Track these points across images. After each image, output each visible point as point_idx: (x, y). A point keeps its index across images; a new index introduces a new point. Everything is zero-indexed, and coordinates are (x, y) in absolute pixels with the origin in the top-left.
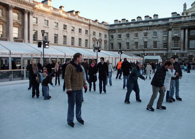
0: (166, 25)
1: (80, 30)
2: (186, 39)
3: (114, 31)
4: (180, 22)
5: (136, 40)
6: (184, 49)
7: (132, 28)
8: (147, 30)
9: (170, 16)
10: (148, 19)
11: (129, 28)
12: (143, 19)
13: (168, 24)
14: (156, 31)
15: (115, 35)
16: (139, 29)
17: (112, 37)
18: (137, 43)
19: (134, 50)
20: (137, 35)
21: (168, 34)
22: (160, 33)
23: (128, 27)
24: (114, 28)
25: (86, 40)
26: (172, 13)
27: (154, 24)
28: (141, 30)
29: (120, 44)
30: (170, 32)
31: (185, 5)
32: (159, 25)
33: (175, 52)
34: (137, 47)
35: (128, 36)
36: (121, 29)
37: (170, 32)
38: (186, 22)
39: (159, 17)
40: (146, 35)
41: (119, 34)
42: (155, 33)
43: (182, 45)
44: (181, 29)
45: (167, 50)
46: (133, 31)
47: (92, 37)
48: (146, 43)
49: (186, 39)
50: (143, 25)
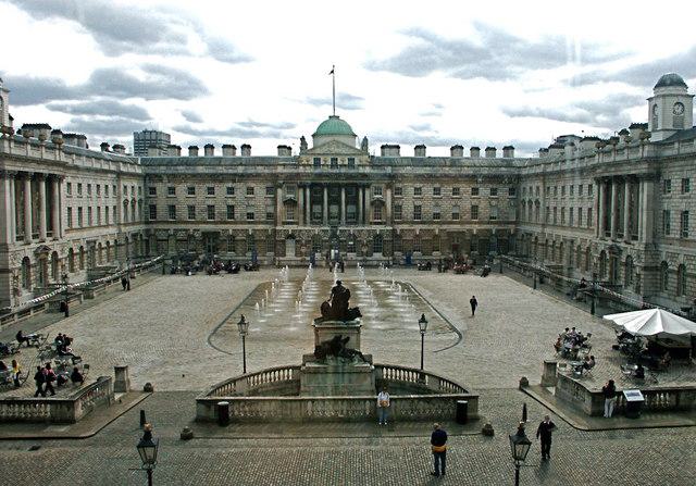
0: (273, 175)
1: (89, 185)
2: (308, 206)
3: (159, 177)
4: (298, 174)
5: (210, 202)
6: (305, 223)
7: (200, 175)
8: (234, 181)
9: (274, 153)
10: (159, 66)
11: (194, 175)
12: (218, 153)
13: (276, 176)
14: (253, 185)
15: (161, 188)
16: (218, 178)
17: (153, 190)
18: (211, 208)
19: (208, 223)
20: (211, 191)
21: (275, 193)
22: (260, 190)
23: (190, 172)
24: (157, 171)
25: (115, 207)
26: (279, 147)
27: (249, 172)
28: (221, 182)
29: (172, 209)
30: (280, 191)
31: (303, 139)
32: (258, 175)
33: (290, 228)
34: (212, 215)
35: (191, 191)
36: (174, 175)
37: (280, 191)
38: (308, 175)
39: (254, 153)
40: (231, 191)
41: (169, 185)
42: (251, 191)
43: (302, 216)
44: (299, 187)
45: (276, 225)
46: (204, 181)
47: (122, 200)
48: (231, 208)
49: (308, 206)
50: (225, 171)
